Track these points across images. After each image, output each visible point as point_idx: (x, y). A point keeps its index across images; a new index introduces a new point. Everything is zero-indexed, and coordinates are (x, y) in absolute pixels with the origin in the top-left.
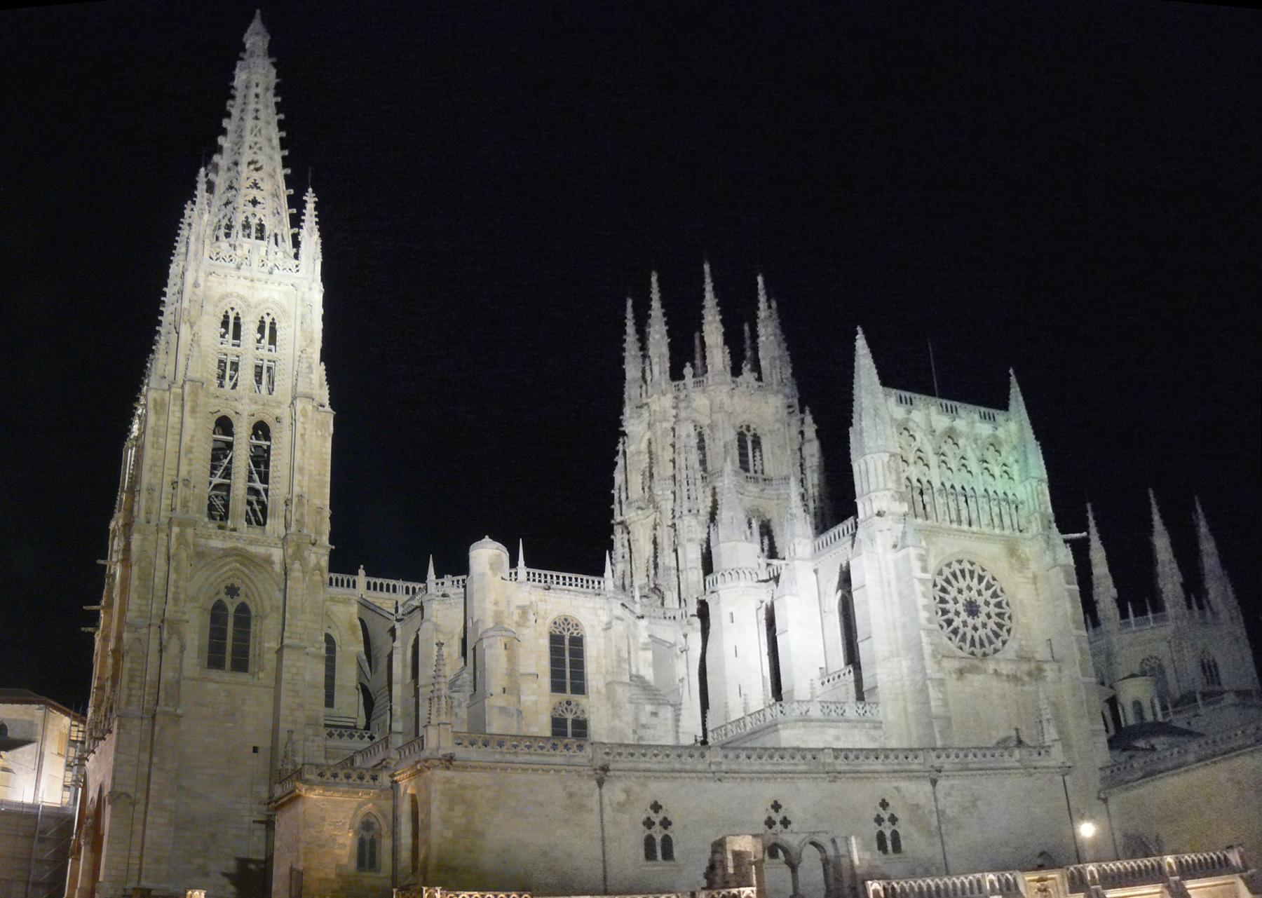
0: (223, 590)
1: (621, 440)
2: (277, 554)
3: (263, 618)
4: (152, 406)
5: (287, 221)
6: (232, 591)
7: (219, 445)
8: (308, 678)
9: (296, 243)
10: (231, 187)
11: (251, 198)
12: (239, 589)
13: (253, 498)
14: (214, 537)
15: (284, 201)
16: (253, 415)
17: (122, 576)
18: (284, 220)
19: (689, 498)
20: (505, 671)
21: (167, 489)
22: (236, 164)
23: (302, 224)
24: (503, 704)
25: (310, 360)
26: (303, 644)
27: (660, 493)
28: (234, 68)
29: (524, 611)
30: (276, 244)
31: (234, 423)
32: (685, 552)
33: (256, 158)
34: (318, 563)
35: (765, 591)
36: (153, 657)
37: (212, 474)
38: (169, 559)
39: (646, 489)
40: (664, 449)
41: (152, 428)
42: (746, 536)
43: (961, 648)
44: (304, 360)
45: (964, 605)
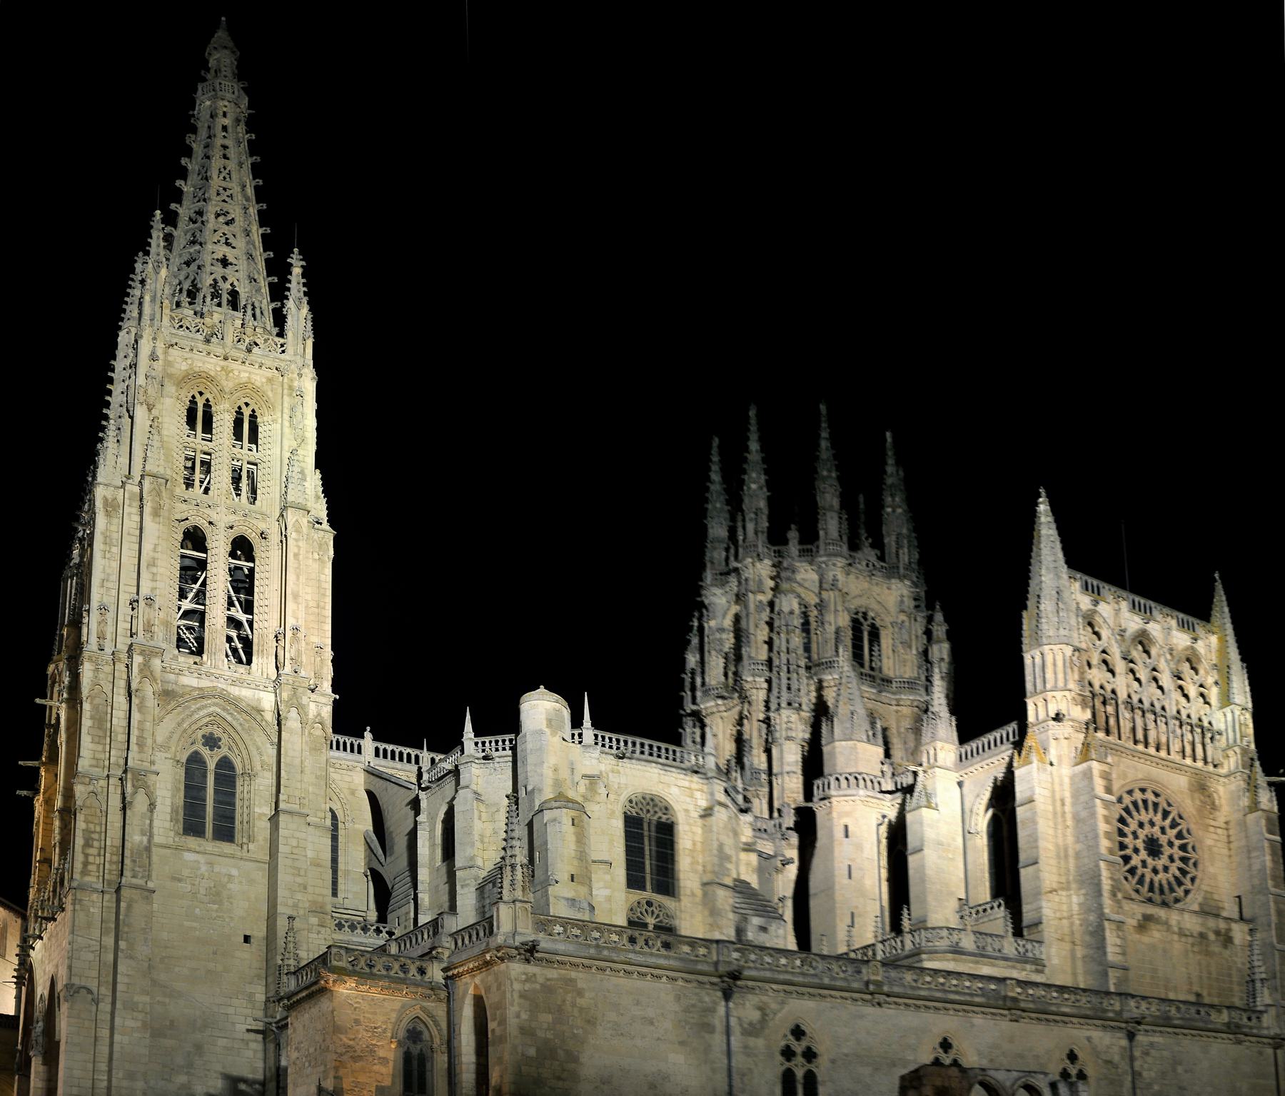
0: (200, 740)
1: (696, 614)
2: (267, 701)
3: (250, 775)
5: (265, 290)
6: (211, 742)
8: (310, 854)
9: (280, 319)
10: (193, 242)
11: (220, 256)
12: (220, 739)
13: (234, 634)
14: (187, 673)
15: (261, 265)
16: (231, 528)
18: (263, 290)
19: (789, 688)
22: (200, 213)
23: (287, 293)
25: (302, 464)
26: (305, 811)
27: (750, 679)
28: (195, 91)
30: (254, 315)
31: (208, 536)
32: (781, 752)
33: (226, 207)
35: (889, 804)
38: (130, 695)
39: (730, 674)
40: (757, 626)
42: (868, 736)
43: (1137, 891)
44: (295, 463)
45: (1144, 841)
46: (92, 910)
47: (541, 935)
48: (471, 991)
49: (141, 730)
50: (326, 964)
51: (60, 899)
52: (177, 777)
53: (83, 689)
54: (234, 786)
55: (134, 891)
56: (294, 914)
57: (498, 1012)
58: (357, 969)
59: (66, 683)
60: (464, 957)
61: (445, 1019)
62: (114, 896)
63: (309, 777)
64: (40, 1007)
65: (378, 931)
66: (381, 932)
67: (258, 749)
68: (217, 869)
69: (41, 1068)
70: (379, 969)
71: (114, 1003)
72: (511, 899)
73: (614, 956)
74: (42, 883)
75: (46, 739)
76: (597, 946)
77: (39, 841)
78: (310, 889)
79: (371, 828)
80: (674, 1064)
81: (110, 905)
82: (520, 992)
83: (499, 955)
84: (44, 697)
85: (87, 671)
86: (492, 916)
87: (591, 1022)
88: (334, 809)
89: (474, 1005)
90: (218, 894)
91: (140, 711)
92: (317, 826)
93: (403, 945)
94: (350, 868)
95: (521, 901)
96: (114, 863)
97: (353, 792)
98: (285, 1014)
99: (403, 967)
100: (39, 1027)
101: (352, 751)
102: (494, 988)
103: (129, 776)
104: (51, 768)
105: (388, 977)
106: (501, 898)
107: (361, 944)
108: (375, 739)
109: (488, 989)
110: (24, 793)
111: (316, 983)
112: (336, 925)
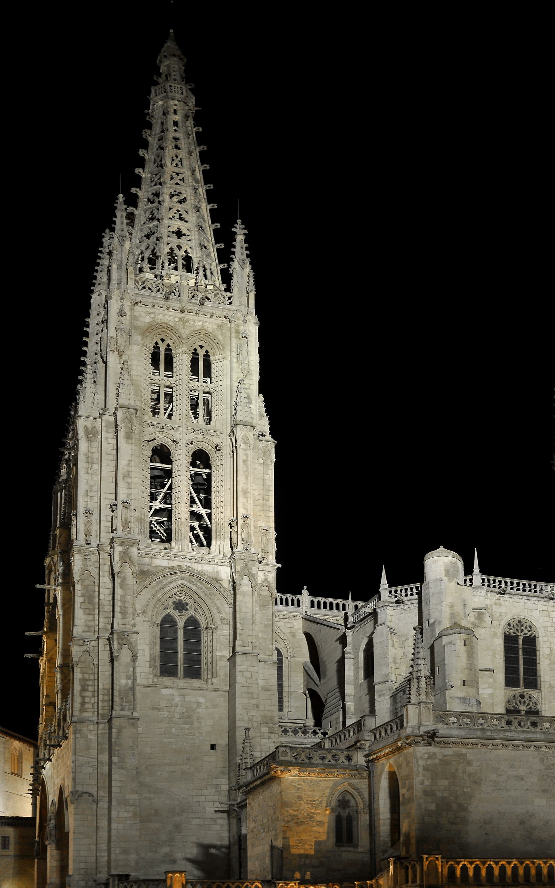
2: (224, 573)
3: (212, 629)
4: (83, 434)
6: (180, 606)
7: (156, 473)
12: (187, 604)
14: (159, 556)
17: (63, 599)
20: (464, 665)
21: (106, 512)
24: (463, 695)
26: (256, 651)
29: (480, 611)
34: (266, 580)
36: (105, 668)
37: (153, 498)
41: (85, 455)
46: (89, 736)
47: (440, 725)
48: (387, 769)
49: (124, 602)
50: (275, 760)
51: (64, 731)
52: (154, 635)
53: (74, 575)
54: (199, 638)
55: (123, 720)
56: (250, 726)
57: (407, 782)
58: (299, 761)
59: (61, 571)
60: (381, 745)
61: (367, 790)
62: (107, 725)
63: (258, 626)
64: (51, 809)
65: (315, 733)
66: (318, 733)
67: (218, 608)
68: (188, 699)
69: (55, 852)
70: (316, 759)
71: (110, 801)
72: (417, 702)
73: (495, 735)
74: (49, 720)
75: (46, 614)
76: (483, 729)
77: (44, 690)
78: (261, 707)
79: (309, 660)
80: (539, 806)
81: (103, 731)
82: (424, 766)
83: (408, 742)
84: (43, 583)
85: (77, 561)
86: (403, 715)
87: (477, 783)
88: (279, 648)
89: (389, 779)
90: (189, 717)
91: (122, 587)
92: (266, 662)
93: (334, 741)
94: (292, 690)
95: (425, 703)
96: (106, 701)
97: (294, 635)
98: (244, 797)
99: (335, 757)
100: (52, 823)
101: (293, 604)
102: (404, 766)
103: (115, 636)
104: (51, 635)
105: (322, 764)
106: (409, 702)
107: (302, 743)
108: (311, 595)
109: (399, 767)
110: (30, 656)
111: (267, 773)
112: (282, 731)
